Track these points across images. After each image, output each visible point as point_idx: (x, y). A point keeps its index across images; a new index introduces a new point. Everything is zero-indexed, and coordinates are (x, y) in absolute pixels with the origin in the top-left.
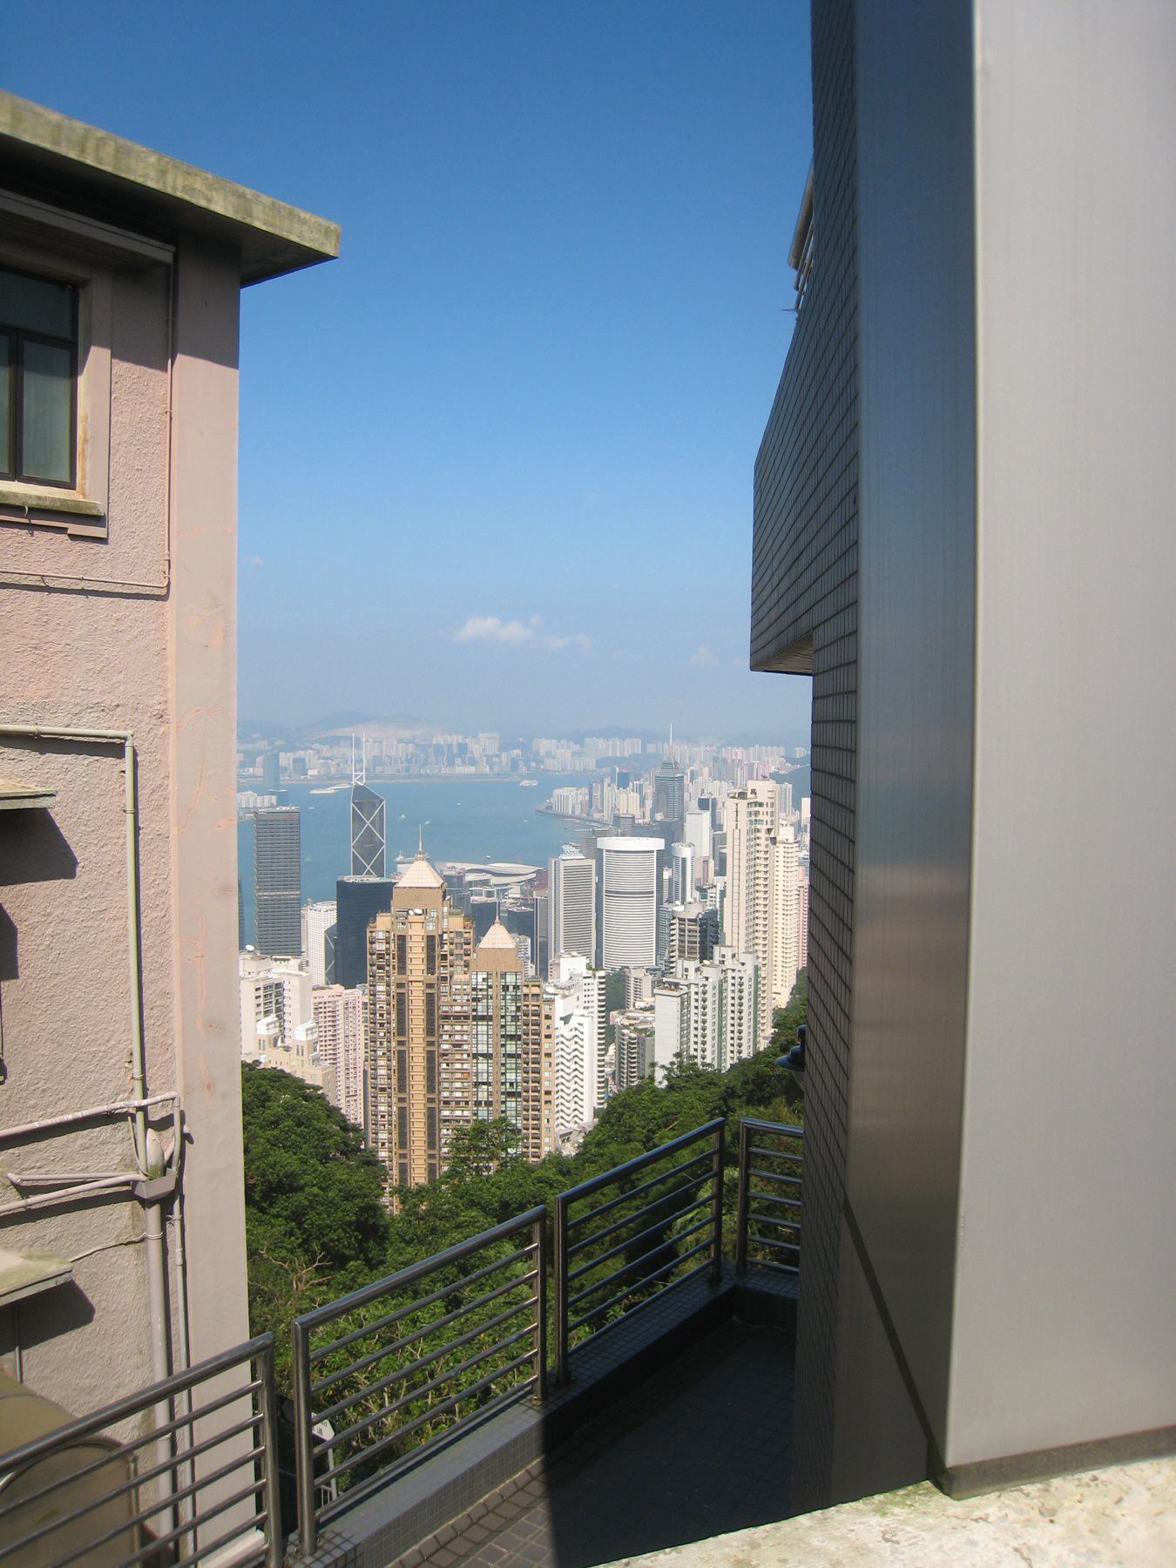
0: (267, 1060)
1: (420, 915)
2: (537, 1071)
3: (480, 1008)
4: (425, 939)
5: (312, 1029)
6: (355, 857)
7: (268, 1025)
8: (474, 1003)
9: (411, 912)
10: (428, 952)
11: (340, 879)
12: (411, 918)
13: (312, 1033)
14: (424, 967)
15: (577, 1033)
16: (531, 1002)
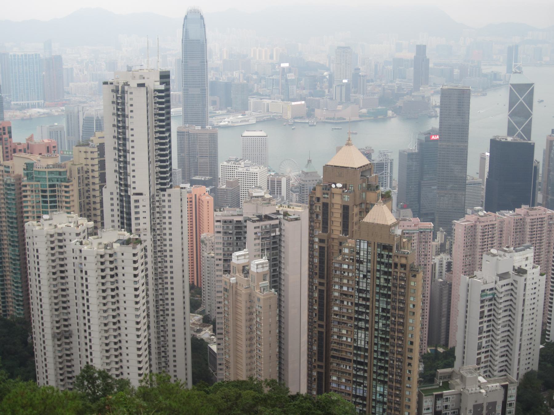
0: (235, 282)
1: (340, 188)
2: (402, 324)
3: (361, 268)
4: (342, 207)
5: (262, 264)
6: (509, 122)
7: (238, 256)
8: (357, 265)
9: (333, 186)
10: (343, 219)
11: (492, 137)
12: (334, 191)
13: (263, 267)
14: (340, 229)
15: (512, 287)
16: (399, 268)
